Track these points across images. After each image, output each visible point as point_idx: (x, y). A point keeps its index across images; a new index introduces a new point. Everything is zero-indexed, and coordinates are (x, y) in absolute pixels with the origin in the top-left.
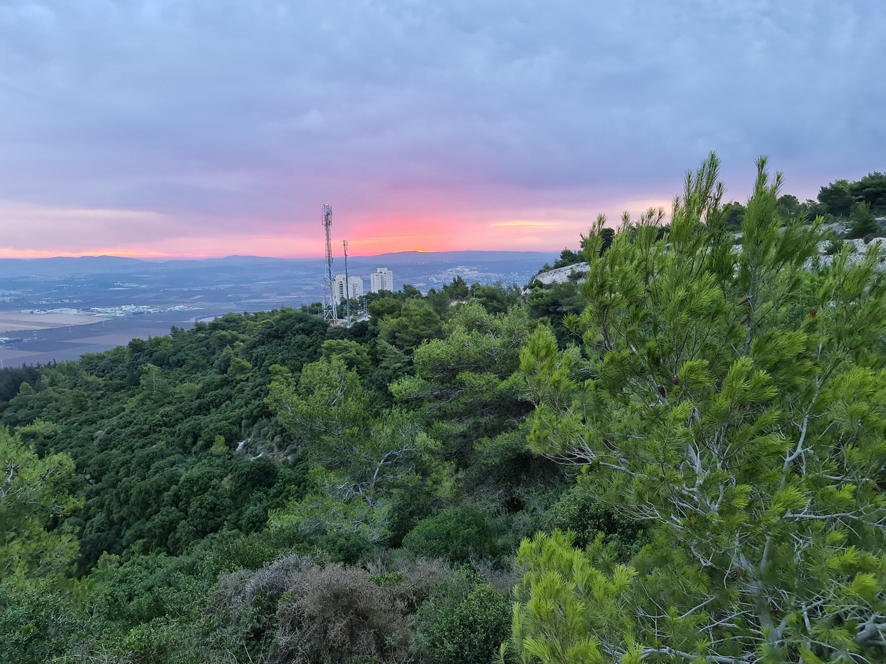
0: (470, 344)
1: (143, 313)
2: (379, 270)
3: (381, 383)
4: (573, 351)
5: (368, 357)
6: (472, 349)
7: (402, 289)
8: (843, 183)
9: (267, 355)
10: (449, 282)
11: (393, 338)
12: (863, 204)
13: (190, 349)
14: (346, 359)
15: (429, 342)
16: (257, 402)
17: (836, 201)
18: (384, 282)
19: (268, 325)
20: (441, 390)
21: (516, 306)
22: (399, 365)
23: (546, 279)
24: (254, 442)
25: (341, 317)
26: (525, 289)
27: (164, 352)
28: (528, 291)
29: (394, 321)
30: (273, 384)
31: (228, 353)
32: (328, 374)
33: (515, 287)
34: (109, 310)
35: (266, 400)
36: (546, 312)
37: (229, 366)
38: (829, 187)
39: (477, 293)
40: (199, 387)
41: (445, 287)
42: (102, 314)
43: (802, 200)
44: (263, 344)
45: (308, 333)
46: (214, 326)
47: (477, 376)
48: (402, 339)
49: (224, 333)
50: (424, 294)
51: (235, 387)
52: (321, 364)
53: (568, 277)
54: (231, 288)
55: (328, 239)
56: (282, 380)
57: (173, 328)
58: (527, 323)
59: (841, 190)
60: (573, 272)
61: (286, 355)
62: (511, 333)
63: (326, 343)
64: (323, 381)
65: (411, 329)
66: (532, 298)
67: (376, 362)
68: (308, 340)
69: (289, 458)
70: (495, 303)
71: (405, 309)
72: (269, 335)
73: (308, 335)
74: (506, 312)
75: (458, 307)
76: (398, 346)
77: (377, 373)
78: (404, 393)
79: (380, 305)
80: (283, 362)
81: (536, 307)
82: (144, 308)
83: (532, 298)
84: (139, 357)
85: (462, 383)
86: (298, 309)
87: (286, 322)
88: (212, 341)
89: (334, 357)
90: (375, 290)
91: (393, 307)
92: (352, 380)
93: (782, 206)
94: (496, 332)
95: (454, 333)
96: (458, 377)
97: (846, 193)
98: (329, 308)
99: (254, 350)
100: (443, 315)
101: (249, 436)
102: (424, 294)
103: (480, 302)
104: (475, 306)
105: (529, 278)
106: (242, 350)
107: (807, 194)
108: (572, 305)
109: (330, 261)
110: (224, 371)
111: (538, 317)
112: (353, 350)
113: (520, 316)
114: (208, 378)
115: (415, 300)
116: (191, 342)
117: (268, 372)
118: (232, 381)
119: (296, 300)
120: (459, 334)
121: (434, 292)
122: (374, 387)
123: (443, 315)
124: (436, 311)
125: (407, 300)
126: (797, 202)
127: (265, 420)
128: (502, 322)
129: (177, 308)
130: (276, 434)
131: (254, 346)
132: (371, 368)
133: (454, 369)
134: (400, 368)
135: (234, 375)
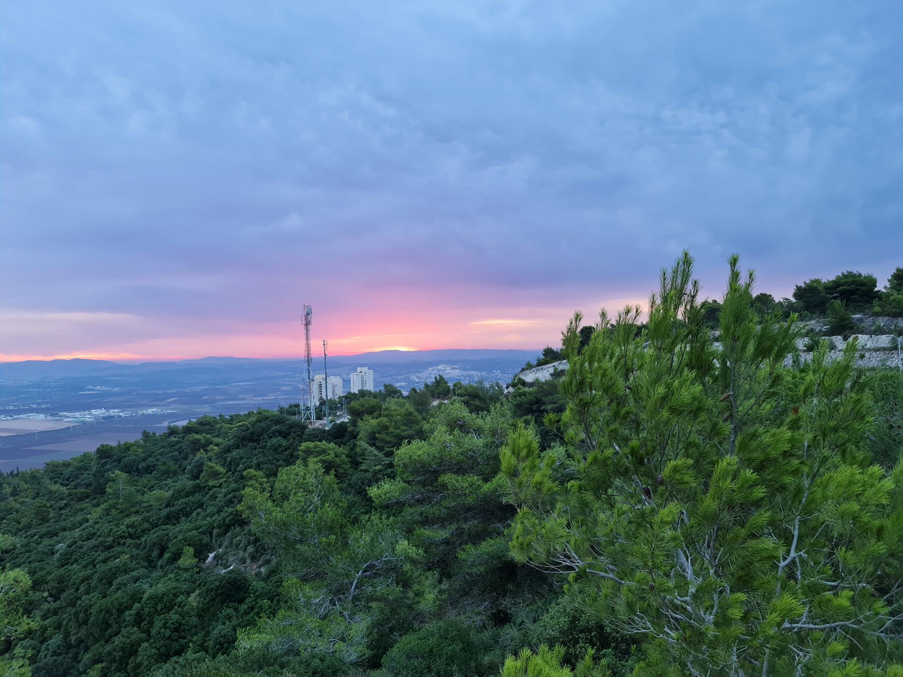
0: (452, 445)
1: (113, 417)
2: (359, 369)
3: (361, 487)
4: (557, 452)
5: (346, 460)
6: (455, 450)
7: (382, 388)
8: (817, 281)
9: (241, 458)
10: (431, 381)
11: (373, 439)
12: (839, 301)
13: (161, 454)
14: (324, 462)
15: (409, 443)
16: (230, 510)
17: (811, 299)
18: (364, 381)
19: (244, 428)
20: (422, 493)
21: (498, 405)
22: (379, 467)
23: (529, 377)
24: (225, 553)
25: (319, 418)
26: (507, 388)
27: (133, 457)
28: (511, 390)
29: (374, 422)
30: (248, 490)
31: (201, 458)
32: (304, 479)
33: (498, 385)
34: (78, 414)
35: (239, 507)
36: (530, 411)
37: (202, 471)
38: (803, 285)
39: (460, 391)
40: (169, 494)
41: (427, 386)
42: (70, 419)
43: (778, 298)
44: (238, 448)
45: (285, 435)
46: (188, 430)
47: (460, 478)
48: (383, 440)
50: (405, 393)
51: (207, 493)
52: (298, 468)
53: (551, 375)
54: (207, 389)
55: (307, 339)
56: (257, 485)
57: (145, 432)
58: (510, 422)
59: (815, 289)
60: (555, 369)
61: (262, 459)
62: (494, 433)
63: (303, 446)
64: (299, 486)
65: (391, 429)
66: (515, 397)
67: (355, 464)
68: (285, 443)
69: (262, 569)
70: (477, 402)
71: (386, 409)
72: (244, 438)
73: (284, 437)
74: (488, 411)
75: (439, 406)
76: (378, 448)
77: (355, 477)
78: (383, 497)
79: (360, 405)
80: (258, 467)
81: (519, 406)
82: (114, 412)
83: (515, 397)
84: (106, 463)
85: (444, 486)
86: (275, 410)
87: (262, 425)
88: (185, 445)
89: (312, 460)
90: (355, 390)
91: (373, 407)
92: (330, 484)
93: (759, 304)
94: (479, 431)
95: (436, 433)
96: (440, 480)
97: (820, 292)
98: (308, 409)
99: (228, 454)
100: (424, 414)
101: (220, 546)
102: (405, 393)
103: (463, 401)
104: (457, 405)
105: (511, 376)
106: (216, 455)
107: (783, 293)
108: (555, 403)
109: (309, 361)
110: (196, 477)
111: (521, 416)
112: (332, 452)
113: (503, 415)
114: (178, 485)
115: (396, 400)
116: (162, 447)
117: (242, 477)
118: (204, 487)
119: (272, 401)
120: (441, 434)
121: (416, 391)
122: (353, 491)
123: (424, 414)
124: (417, 410)
125: (388, 399)
126: (772, 300)
127: (238, 529)
128: (485, 422)
129: (150, 411)
130: (249, 543)
131: (228, 450)
132: (350, 471)
133: (435, 471)
134: (380, 471)
135: (207, 481)
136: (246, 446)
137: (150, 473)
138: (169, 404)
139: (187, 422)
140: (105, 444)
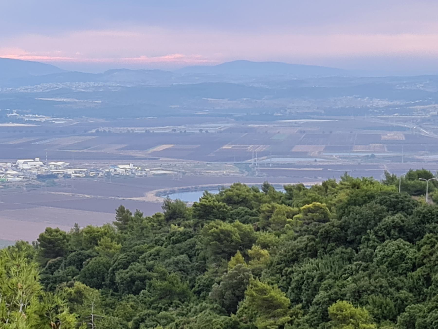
1: (55, 176)
9: (322, 278)
27: (104, 259)
37: (241, 297)
44: (314, 255)
45: (412, 236)
46: (205, 212)
49: (226, 226)
57: (121, 211)
61: (364, 283)
68: (411, 252)
72: (327, 236)
80: (358, 297)
82: (57, 166)
84: (56, 266)
87: (365, 210)
88: (200, 241)
99: (295, 267)
110: (230, 308)
116: (157, 242)
129: (121, 169)
131: (294, 259)
136: (331, 252)
137: (136, 293)
138: (156, 157)
139: (200, 195)
140: (54, 228)
